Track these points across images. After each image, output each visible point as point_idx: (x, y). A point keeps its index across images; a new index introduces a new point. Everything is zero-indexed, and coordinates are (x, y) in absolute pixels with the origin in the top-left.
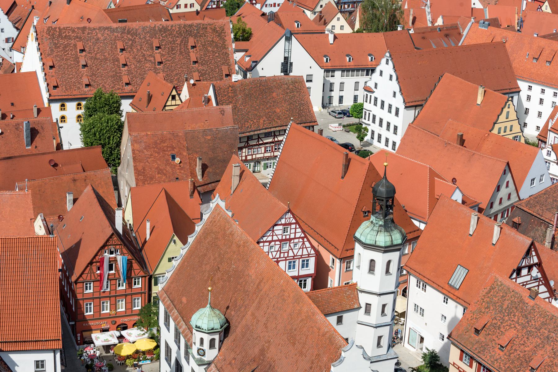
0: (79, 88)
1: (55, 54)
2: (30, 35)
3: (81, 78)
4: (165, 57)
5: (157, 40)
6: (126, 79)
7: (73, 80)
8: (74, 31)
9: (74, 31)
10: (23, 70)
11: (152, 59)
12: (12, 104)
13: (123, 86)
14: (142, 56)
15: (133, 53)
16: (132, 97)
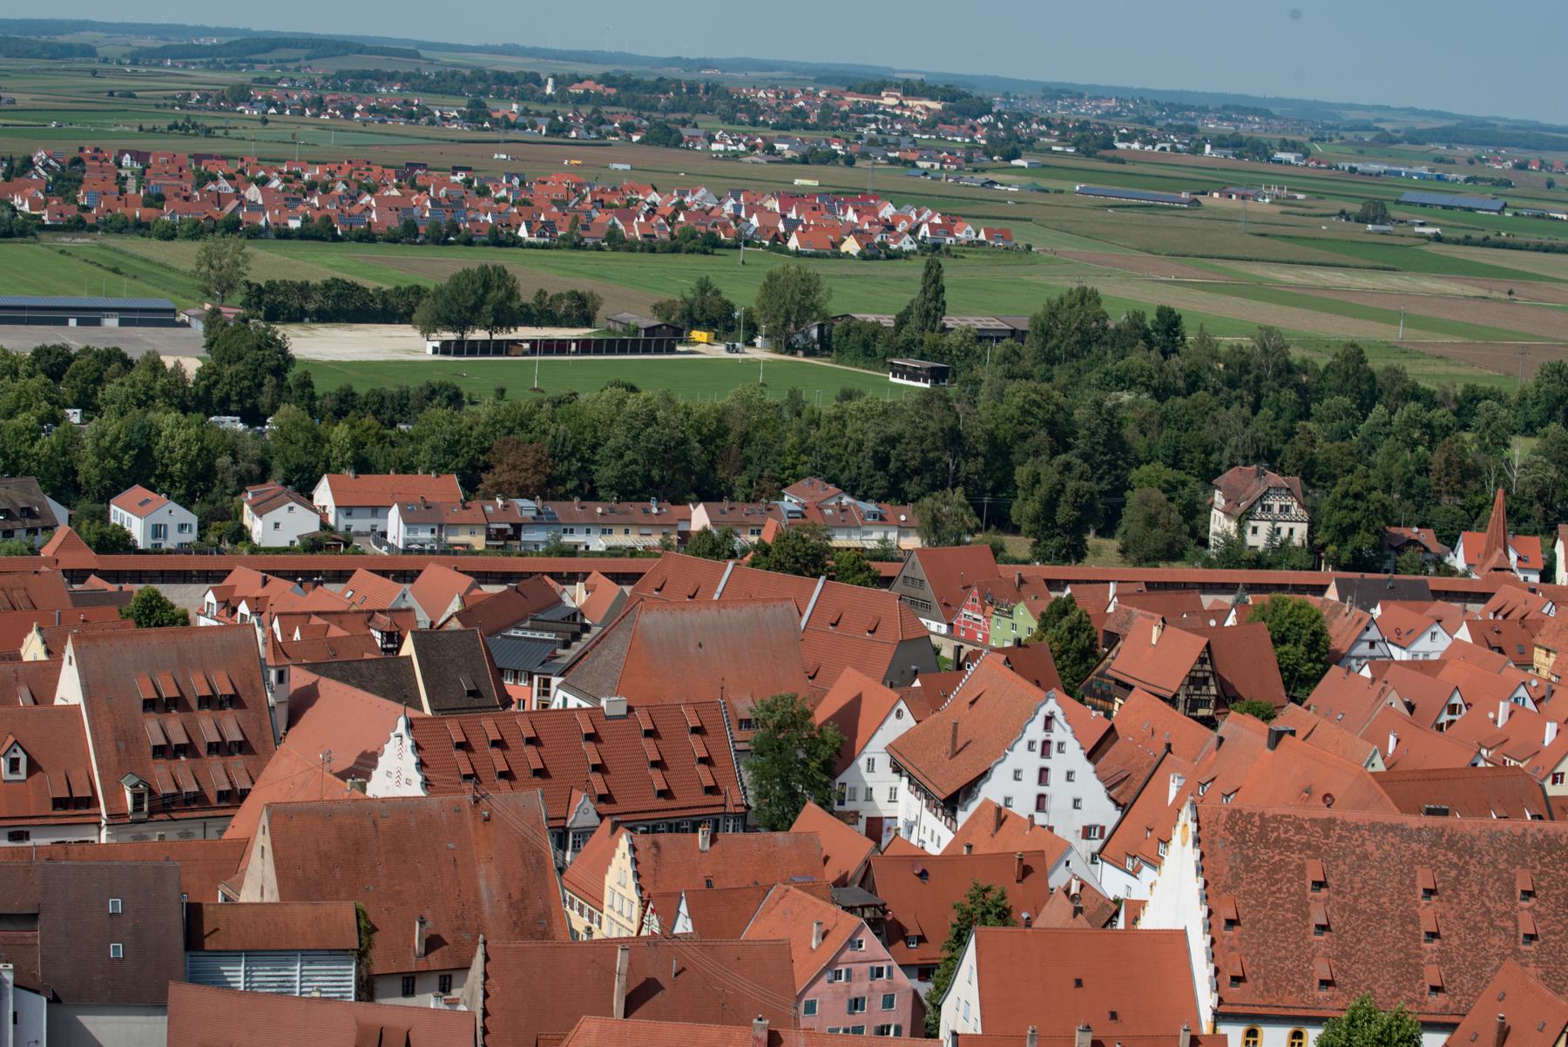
0: (1301, 989)
1: (1244, 886)
2: (1179, 828)
3: (1309, 961)
4: (1546, 923)
5: (1527, 873)
6: (1432, 976)
7: (1289, 964)
8: (1300, 828)
9: (1300, 828)
10: (1147, 922)
11: (1510, 924)
12: (1114, 1016)
13: (1422, 994)
14: (1483, 914)
15: (1459, 903)
16: (1449, 1027)
